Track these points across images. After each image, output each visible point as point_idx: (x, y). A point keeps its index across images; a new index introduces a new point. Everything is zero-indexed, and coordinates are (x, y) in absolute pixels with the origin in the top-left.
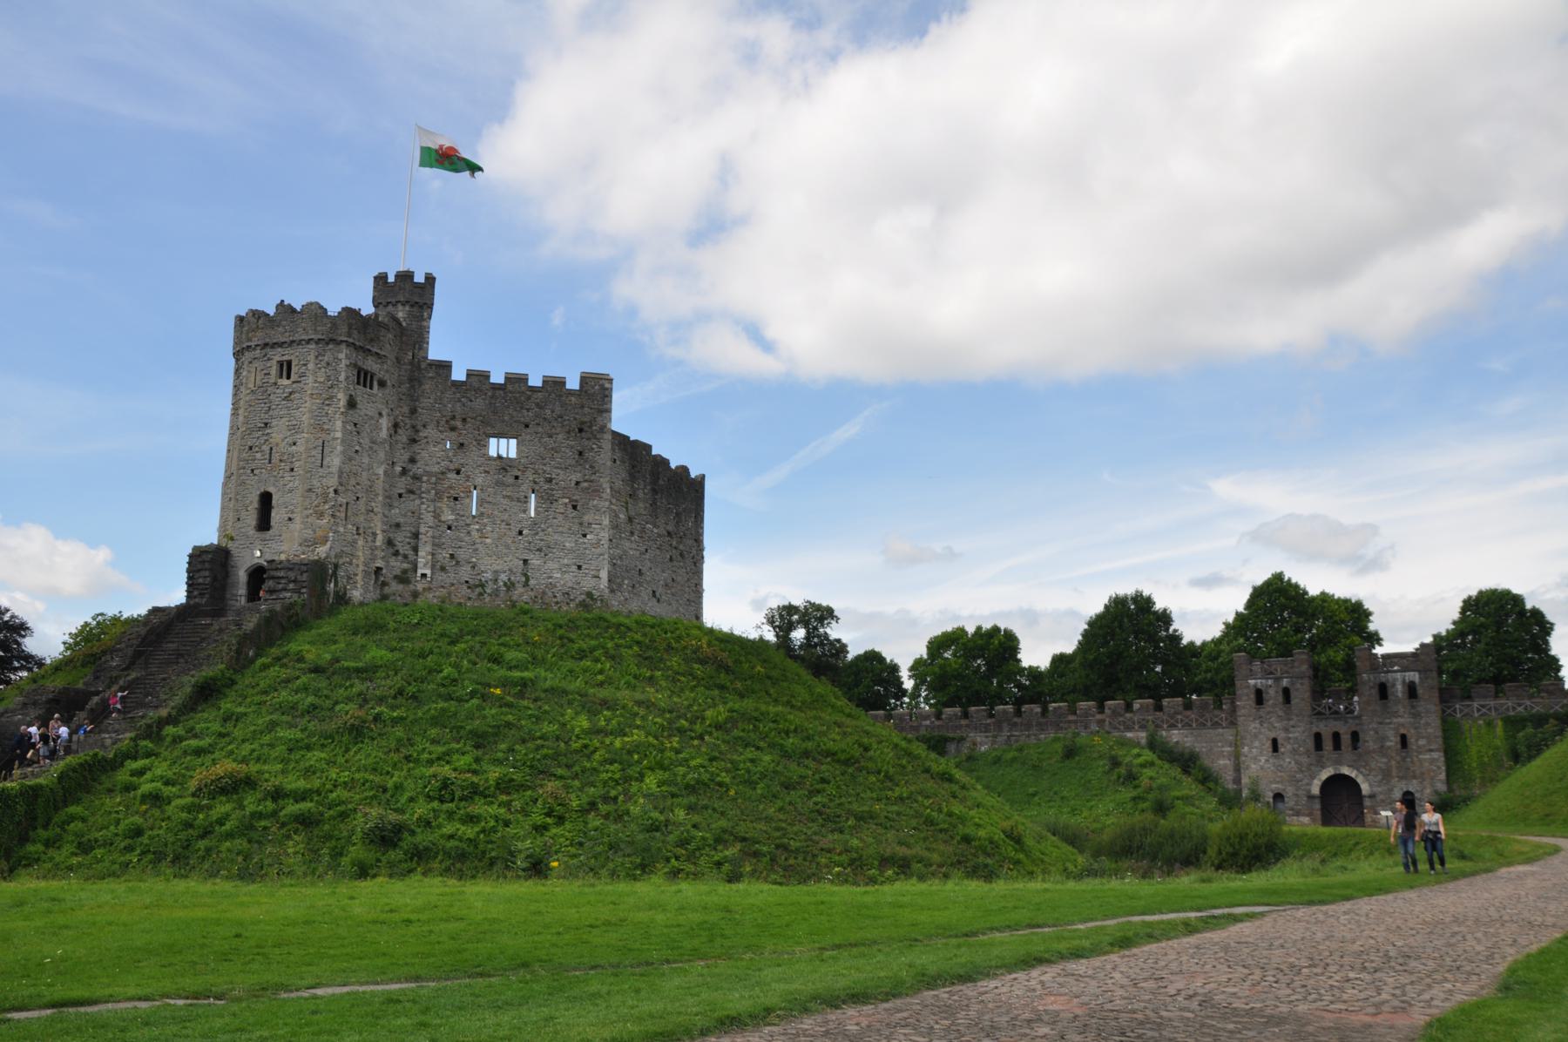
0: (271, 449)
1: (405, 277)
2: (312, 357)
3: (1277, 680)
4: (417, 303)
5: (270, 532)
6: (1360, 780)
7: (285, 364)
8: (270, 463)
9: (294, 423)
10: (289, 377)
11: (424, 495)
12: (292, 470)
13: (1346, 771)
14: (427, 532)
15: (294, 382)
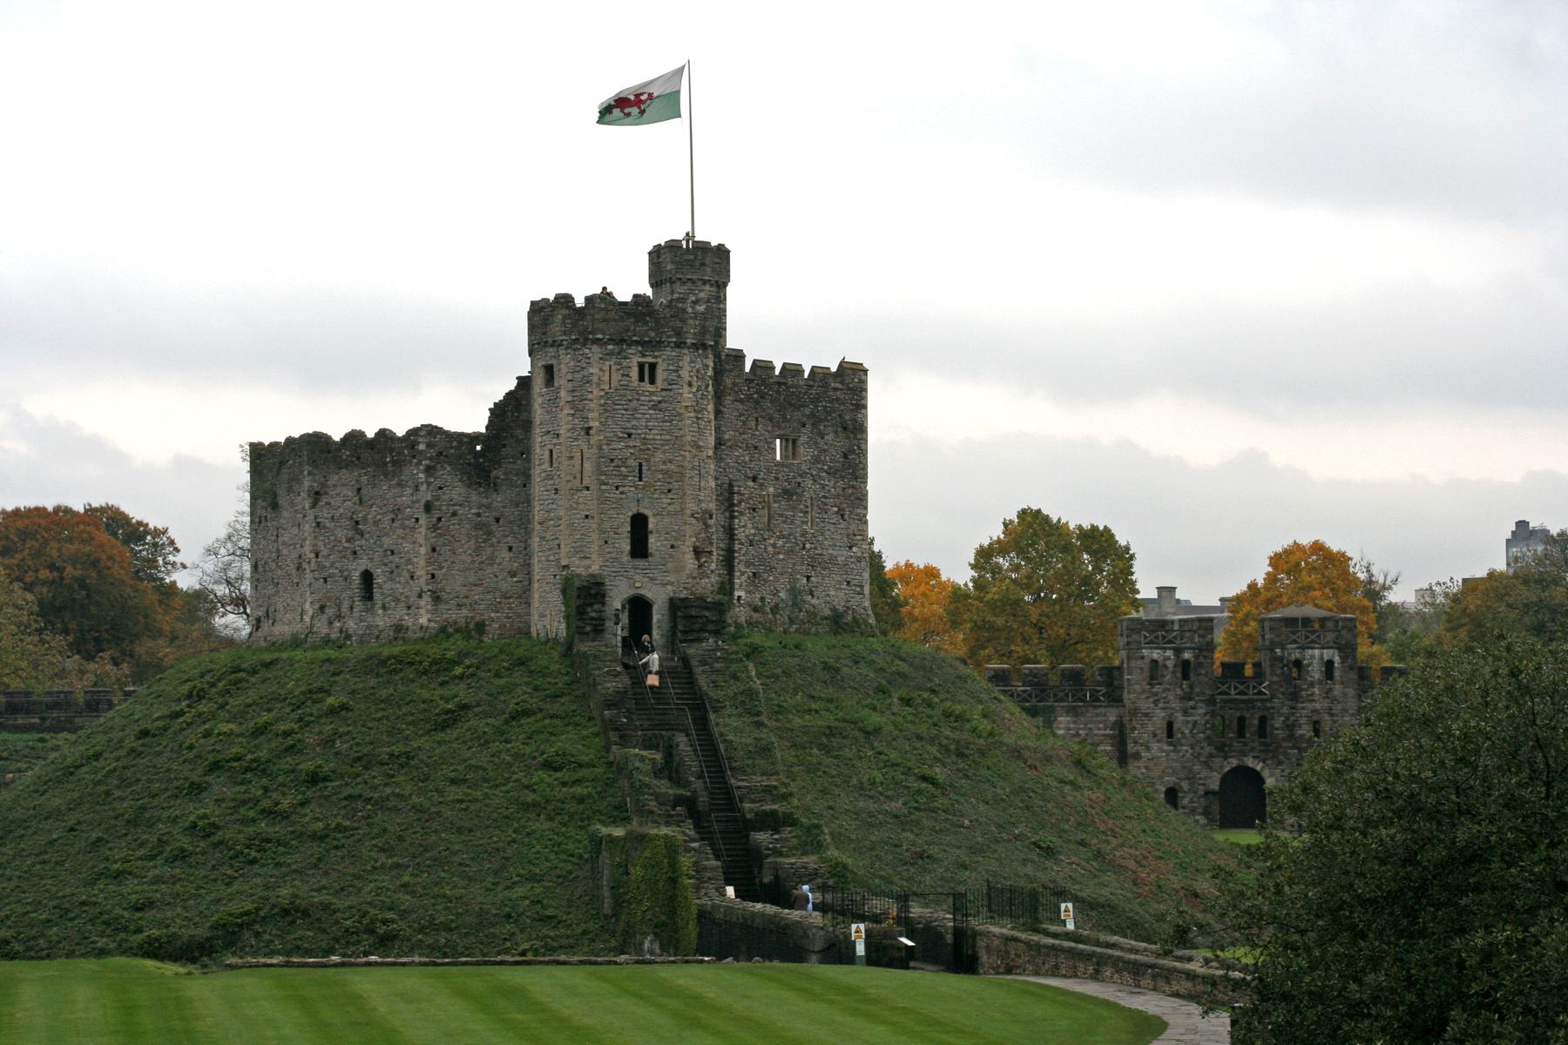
0: (640, 465)
1: (703, 247)
2: (687, 359)
3: (1178, 651)
4: (717, 282)
5: (650, 559)
6: (1265, 774)
7: (647, 367)
8: (640, 480)
9: (668, 437)
10: (652, 381)
11: (736, 508)
12: (669, 491)
13: (1250, 762)
14: (740, 549)
15: (662, 390)
